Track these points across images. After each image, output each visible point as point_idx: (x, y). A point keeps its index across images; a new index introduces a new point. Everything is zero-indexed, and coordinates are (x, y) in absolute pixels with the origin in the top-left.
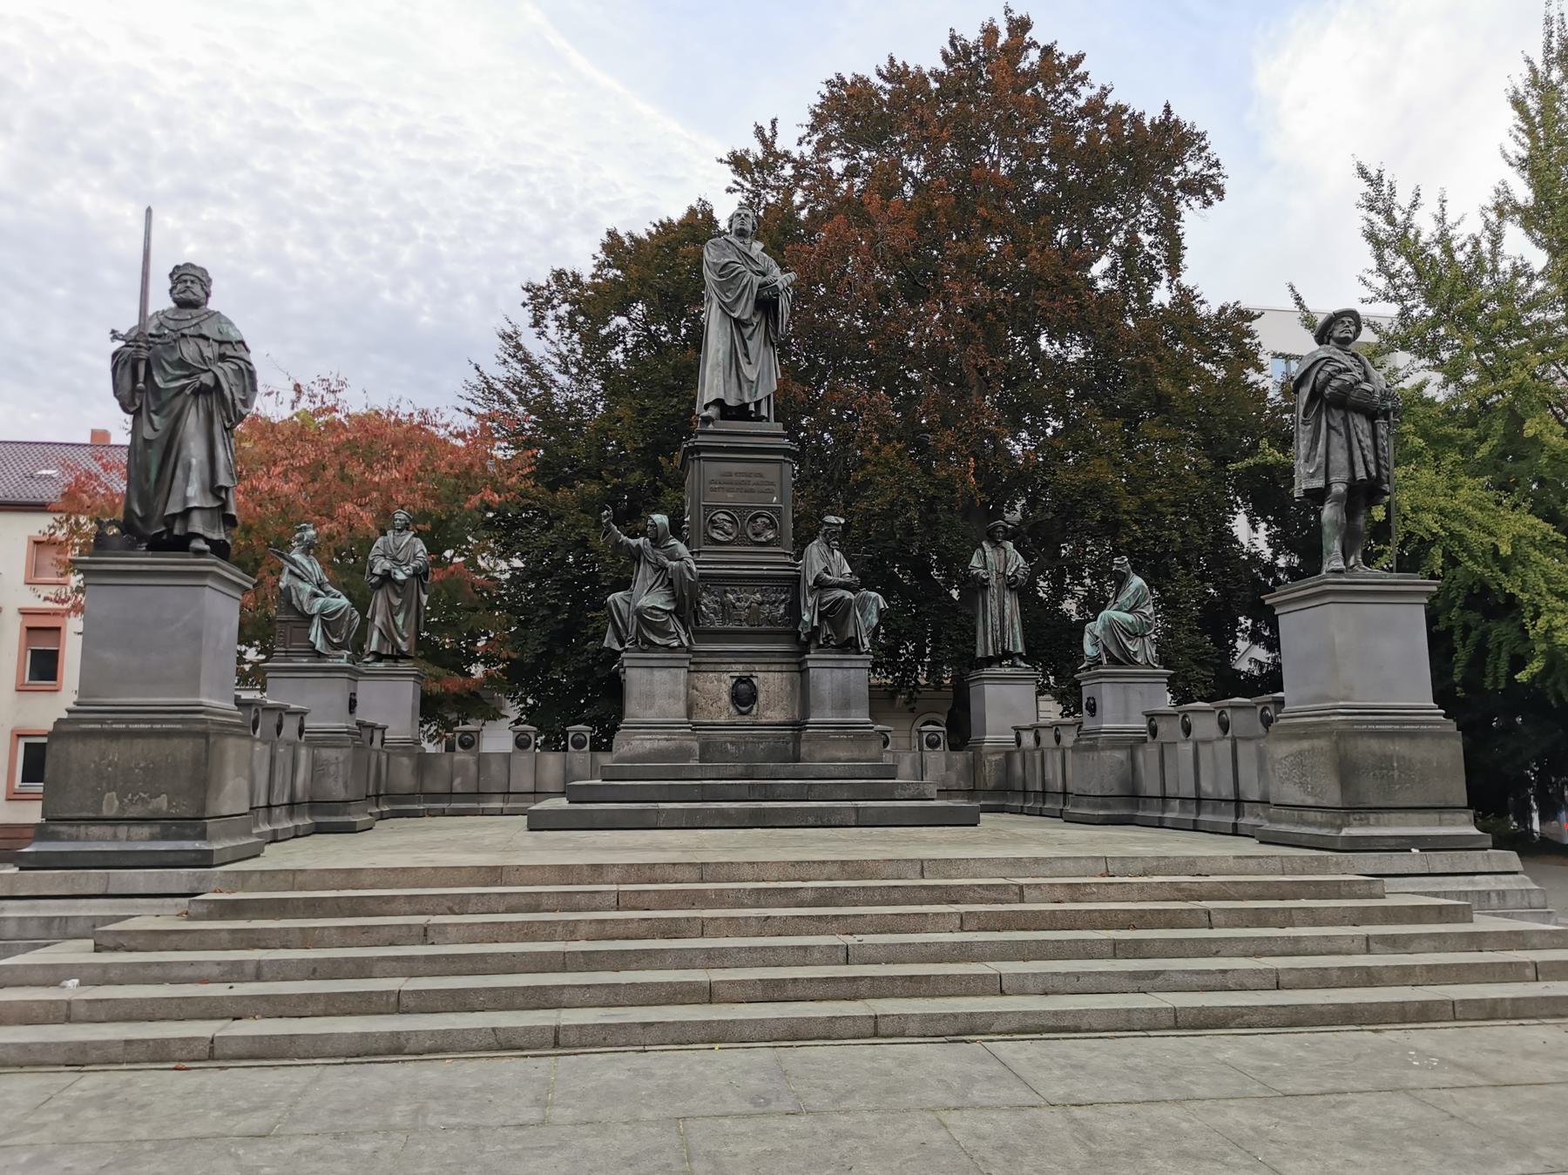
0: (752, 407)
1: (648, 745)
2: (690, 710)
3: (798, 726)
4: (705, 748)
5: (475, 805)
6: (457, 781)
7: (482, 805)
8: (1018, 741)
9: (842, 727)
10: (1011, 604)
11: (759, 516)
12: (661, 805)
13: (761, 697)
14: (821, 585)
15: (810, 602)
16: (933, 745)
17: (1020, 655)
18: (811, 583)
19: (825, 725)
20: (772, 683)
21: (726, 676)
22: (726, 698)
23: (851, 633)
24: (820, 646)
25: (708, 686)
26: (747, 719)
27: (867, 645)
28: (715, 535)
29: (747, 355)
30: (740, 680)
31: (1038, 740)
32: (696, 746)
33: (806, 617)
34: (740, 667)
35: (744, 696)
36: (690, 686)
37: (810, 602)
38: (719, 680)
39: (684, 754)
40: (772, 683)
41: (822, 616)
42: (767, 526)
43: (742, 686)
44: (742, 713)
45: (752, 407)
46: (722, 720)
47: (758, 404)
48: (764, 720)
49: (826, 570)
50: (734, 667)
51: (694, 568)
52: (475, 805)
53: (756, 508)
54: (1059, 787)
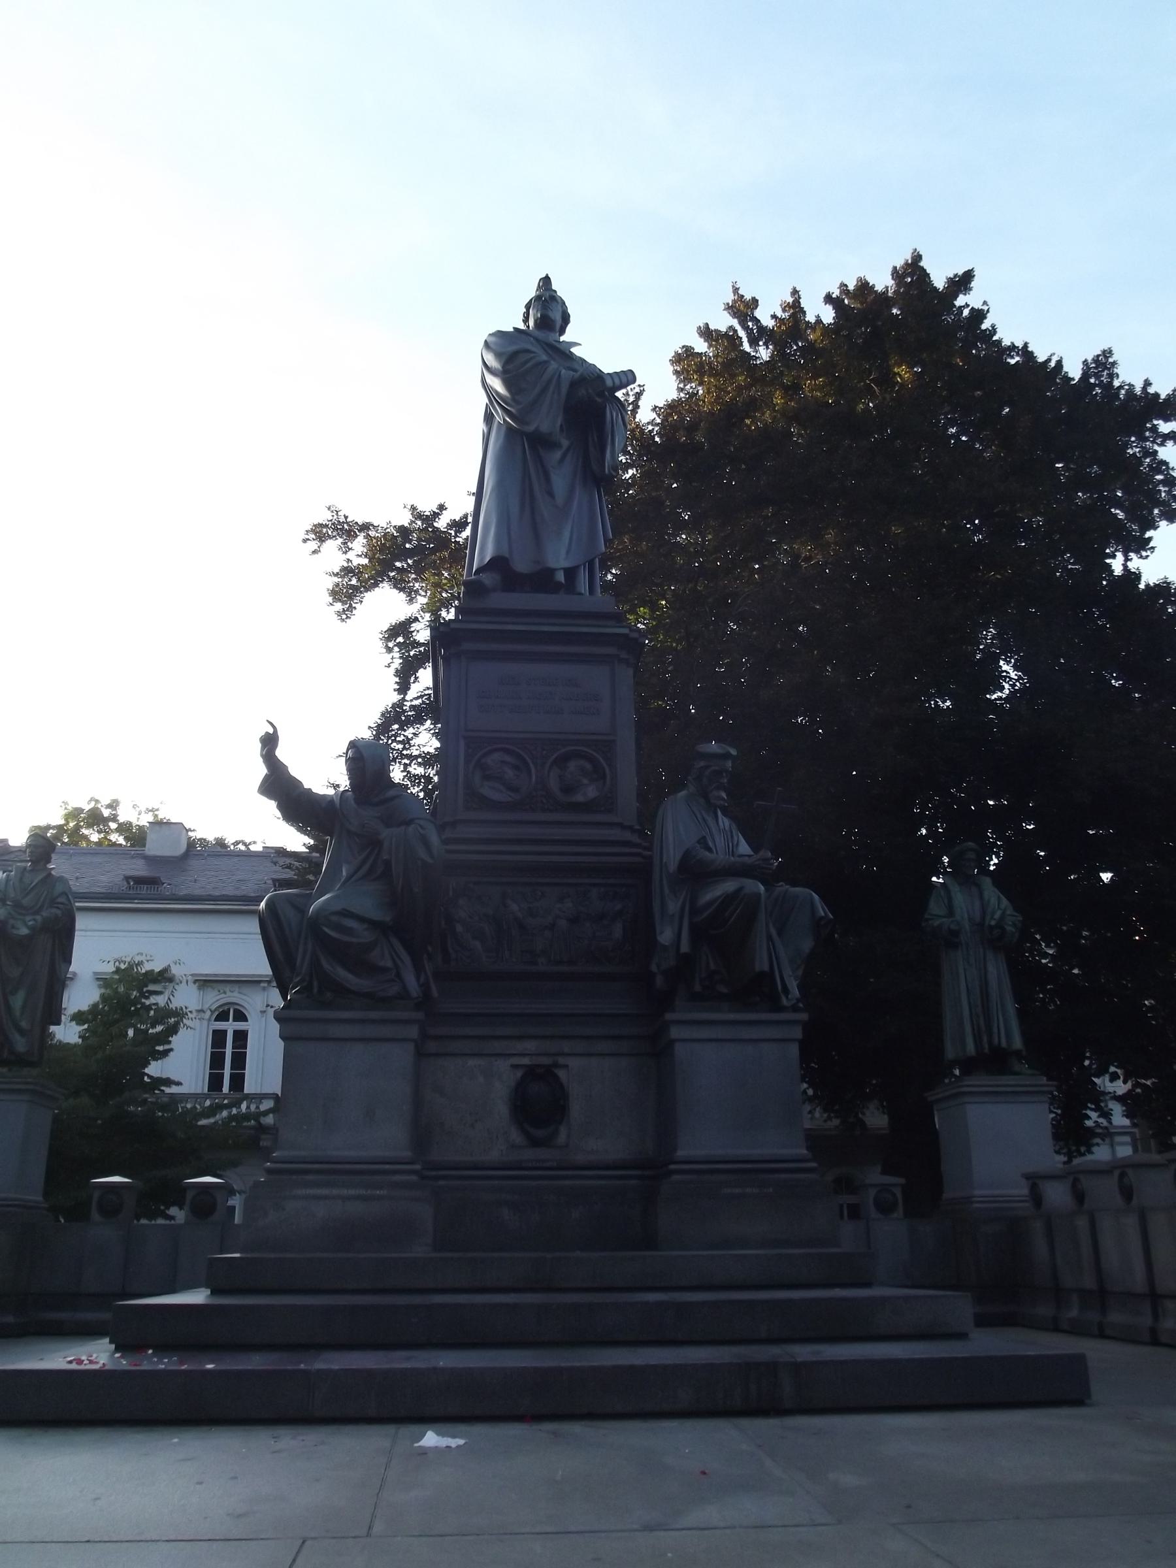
3: (653, 1168)
8: (1036, 1198)
10: (996, 970)
13: (576, 1109)
14: (694, 872)
15: (673, 906)
16: (885, 1208)
17: (1017, 1053)
20: (594, 1079)
21: (503, 1065)
22: (502, 1109)
23: (761, 963)
27: (795, 992)
30: (532, 1074)
31: (1080, 1197)
33: (666, 936)
34: (530, 1046)
37: (673, 906)
40: (594, 1079)
44: (535, 1143)
49: (703, 842)
50: (521, 1046)
51: (434, 839)
54: (1139, 1282)
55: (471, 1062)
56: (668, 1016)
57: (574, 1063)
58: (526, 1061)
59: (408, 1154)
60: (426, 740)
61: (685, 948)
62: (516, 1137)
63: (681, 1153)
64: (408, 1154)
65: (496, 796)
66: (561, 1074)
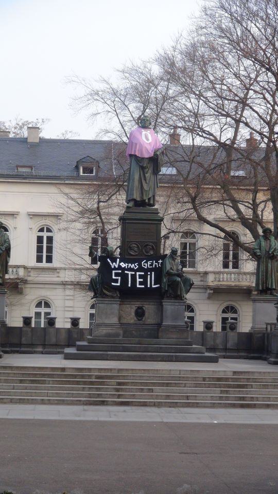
0: (147, 201)
1: (104, 331)
2: (120, 319)
4: (125, 332)
5: (31, 349)
6: (23, 339)
7: (34, 349)
9: (175, 327)
11: (147, 245)
12: (109, 353)
13: (146, 314)
18: (165, 273)
19: (168, 326)
21: (134, 306)
24: (168, 297)
25: (127, 310)
26: (141, 322)
28: (132, 253)
29: (145, 180)
30: (139, 308)
32: (121, 332)
34: (139, 303)
35: (140, 313)
36: (120, 310)
37: (165, 280)
38: (131, 308)
39: (117, 335)
41: (169, 286)
42: (151, 249)
43: (140, 310)
44: (139, 320)
45: (147, 201)
46: (132, 321)
47: (149, 199)
48: (147, 323)
49: (171, 269)
52: (31, 349)
53: (147, 242)
55: (128, 306)
56: (163, 301)
57: (146, 306)
58: (138, 306)
59: (118, 323)
60: (119, 250)
61: (166, 289)
62: (135, 318)
63: (163, 324)
64: (118, 323)
65: (133, 254)
66: (144, 308)
